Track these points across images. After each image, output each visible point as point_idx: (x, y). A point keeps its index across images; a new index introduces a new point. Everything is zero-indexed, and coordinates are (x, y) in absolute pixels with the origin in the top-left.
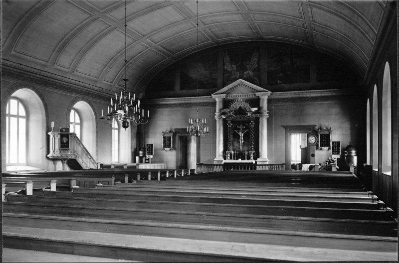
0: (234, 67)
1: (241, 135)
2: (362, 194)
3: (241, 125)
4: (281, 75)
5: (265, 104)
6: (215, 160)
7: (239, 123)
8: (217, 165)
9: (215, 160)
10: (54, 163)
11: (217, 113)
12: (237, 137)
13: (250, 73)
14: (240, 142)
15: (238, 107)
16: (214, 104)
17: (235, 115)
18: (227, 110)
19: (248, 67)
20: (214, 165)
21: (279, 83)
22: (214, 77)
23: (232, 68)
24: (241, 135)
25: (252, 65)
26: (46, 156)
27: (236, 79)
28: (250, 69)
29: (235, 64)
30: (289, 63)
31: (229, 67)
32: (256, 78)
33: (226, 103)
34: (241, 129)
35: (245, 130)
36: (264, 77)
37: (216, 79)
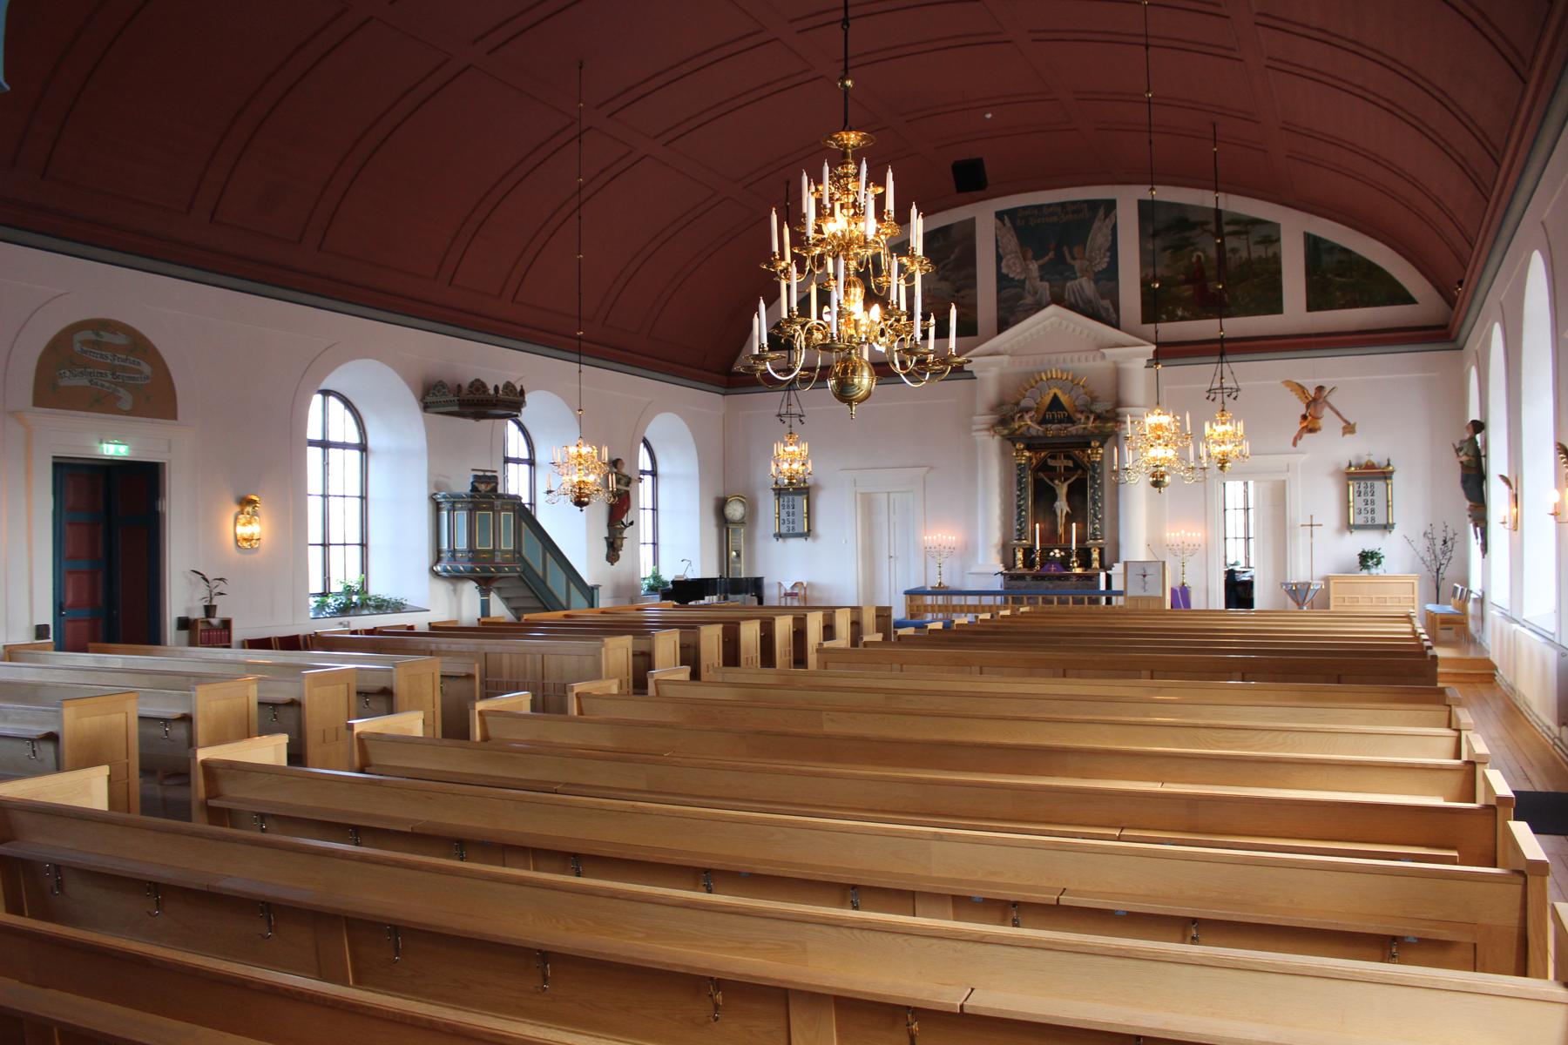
0: (1034, 266)
4: (1187, 291)
10: (455, 591)
15: (1048, 399)
17: (1040, 423)
19: (1077, 264)
23: (1026, 269)
25: (1090, 260)
26: (431, 570)
27: (1038, 307)
28: (1084, 272)
29: (1036, 258)
30: (1213, 253)
32: (1106, 303)
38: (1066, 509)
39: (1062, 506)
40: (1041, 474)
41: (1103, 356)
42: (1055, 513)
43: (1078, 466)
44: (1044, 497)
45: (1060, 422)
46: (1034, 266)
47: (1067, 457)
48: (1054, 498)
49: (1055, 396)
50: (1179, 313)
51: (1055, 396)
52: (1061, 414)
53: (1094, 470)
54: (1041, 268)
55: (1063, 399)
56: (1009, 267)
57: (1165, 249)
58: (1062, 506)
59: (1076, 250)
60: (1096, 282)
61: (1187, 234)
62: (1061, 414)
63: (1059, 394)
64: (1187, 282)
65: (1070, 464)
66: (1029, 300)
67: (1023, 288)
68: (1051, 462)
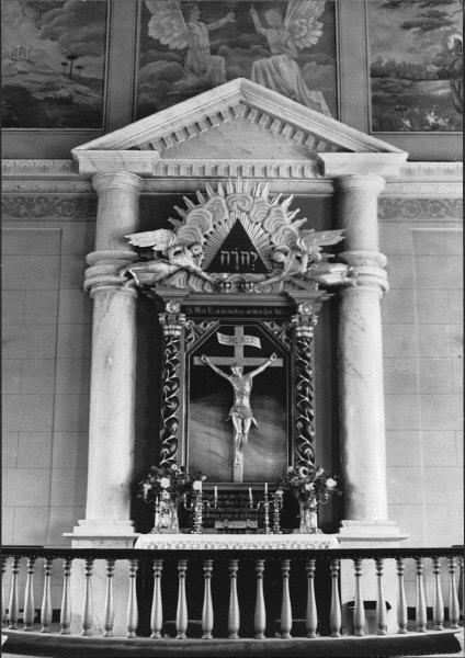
0: (201, 32)
1: (244, 386)
2: (367, 540)
3: (239, 330)
5: (367, 225)
6: (77, 531)
7: (230, 317)
8: (90, 555)
9: (77, 531)
11: (107, 252)
12: (212, 390)
13: (283, 66)
14: (237, 423)
15: (226, 229)
16: (88, 205)
17: (208, 270)
18: (156, 239)
20: (71, 554)
21: (435, 127)
22: (83, 74)
23: (190, 34)
24: (244, 386)
25: (292, 31)
31: (169, 29)
33: (159, 208)
34: (239, 352)
35: (264, 353)
36: (357, 90)
37: (98, 85)
41: (320, 167)
45: (244, 269)
46: (201, 32)
49: (238, 221)
50: (431, 120)
51: (238, 221)
52: (246, 257)
54: (213, 34)
55: (254, 233)
56: (160, 28)
57: (407, 26)
59: (271, 15)
60: (301, 63)
61: (439, 9)
62: (246, 257)
63: (245, 223)
64: (441, 76)
65: (256, 342)
66: (190, 81)
67: (182, 62)
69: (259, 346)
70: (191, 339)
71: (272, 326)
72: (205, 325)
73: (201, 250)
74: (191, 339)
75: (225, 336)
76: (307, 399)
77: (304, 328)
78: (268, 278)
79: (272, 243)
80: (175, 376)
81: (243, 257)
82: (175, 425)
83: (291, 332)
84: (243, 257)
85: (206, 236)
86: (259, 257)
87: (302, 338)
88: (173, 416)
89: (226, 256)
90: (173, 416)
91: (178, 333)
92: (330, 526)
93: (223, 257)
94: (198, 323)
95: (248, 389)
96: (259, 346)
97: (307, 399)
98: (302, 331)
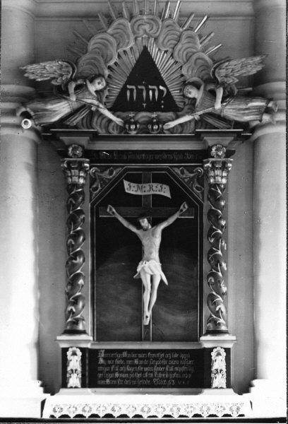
15: (132, 59)
38: (160, 275)
39: (152, 269)
40: (112, 210)
42: (139, 285)
43: (180, 193)
44: (116, 250)
45: (153, 106)
47: (160, 179)
48: (136, 253)
51: (145, 56)
52: (152, 93)
53: (215, 198)
58: (152, 269)
65: (166, 192)
68: (131, 188)
69: (168, 194)
70: (97, 188)
71: (182, 172)
72: (111, 173)
73: (104, 83)
74: (97, 188)
75: (132, 184)
76: (220, 252)
77: (218, 172)
78: (178, 117)
79: (182, 75)
80: (79, 228)
81: (151, 93)
82: (81, 282)
83: (202, 178)
84: (151, 93)
85: (110, 68)
86: (168, 92)
87: (216, 185)
88: (79, 271)
89: (132, 90)
90: (79, 271)
91: (82, 181)
92: (243, 387)
93: (128, 94)
94: (103, 169)
95: (157, 240)
96: (168, 194)
97: (220, 252)
98: (214, 177)
